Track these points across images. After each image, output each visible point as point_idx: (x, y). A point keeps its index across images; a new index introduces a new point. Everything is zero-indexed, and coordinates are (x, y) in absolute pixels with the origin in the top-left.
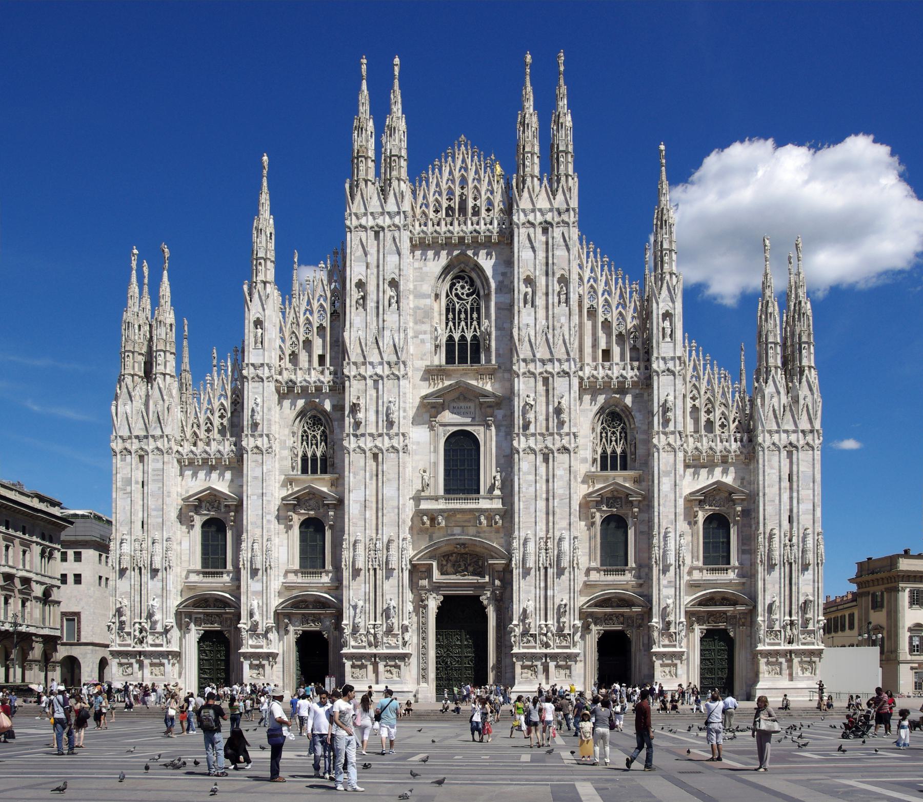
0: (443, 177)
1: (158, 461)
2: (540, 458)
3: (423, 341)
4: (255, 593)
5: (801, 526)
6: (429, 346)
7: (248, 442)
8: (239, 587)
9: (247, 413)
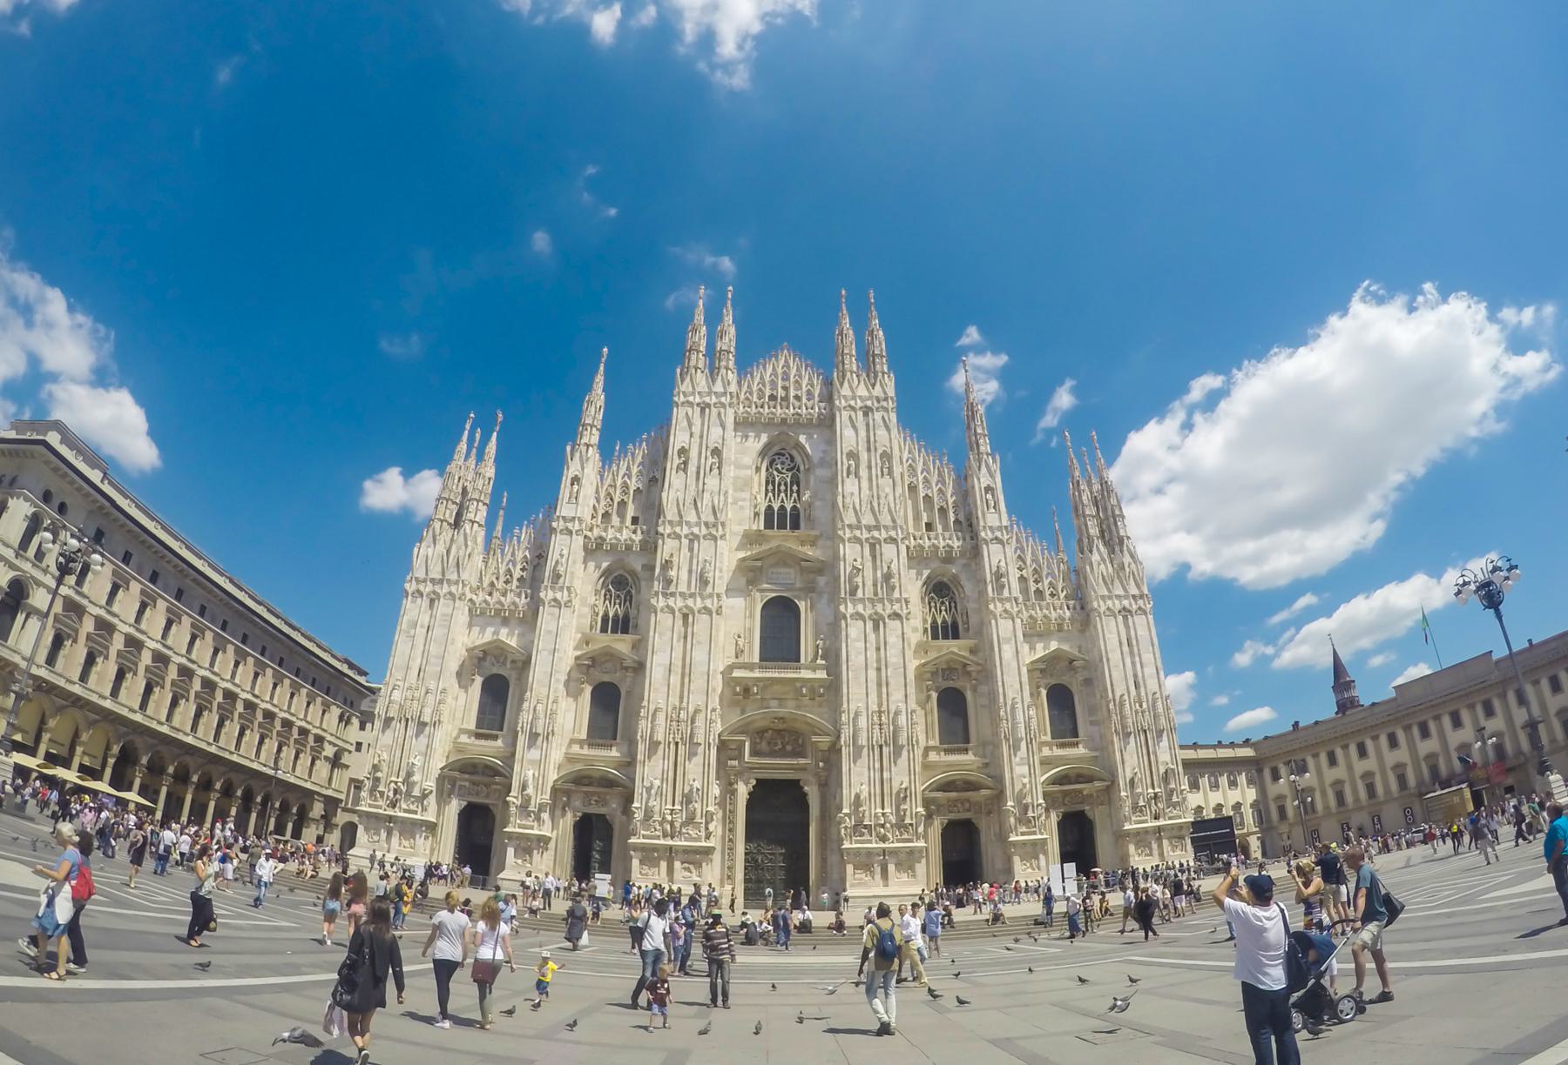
0: (768, 372)
2: (870, 625)
3: (742, 508)
4: (531, 762)
6: (749, 513)
7: (546, 595)
8: (513, 754)
9: (550, 565)
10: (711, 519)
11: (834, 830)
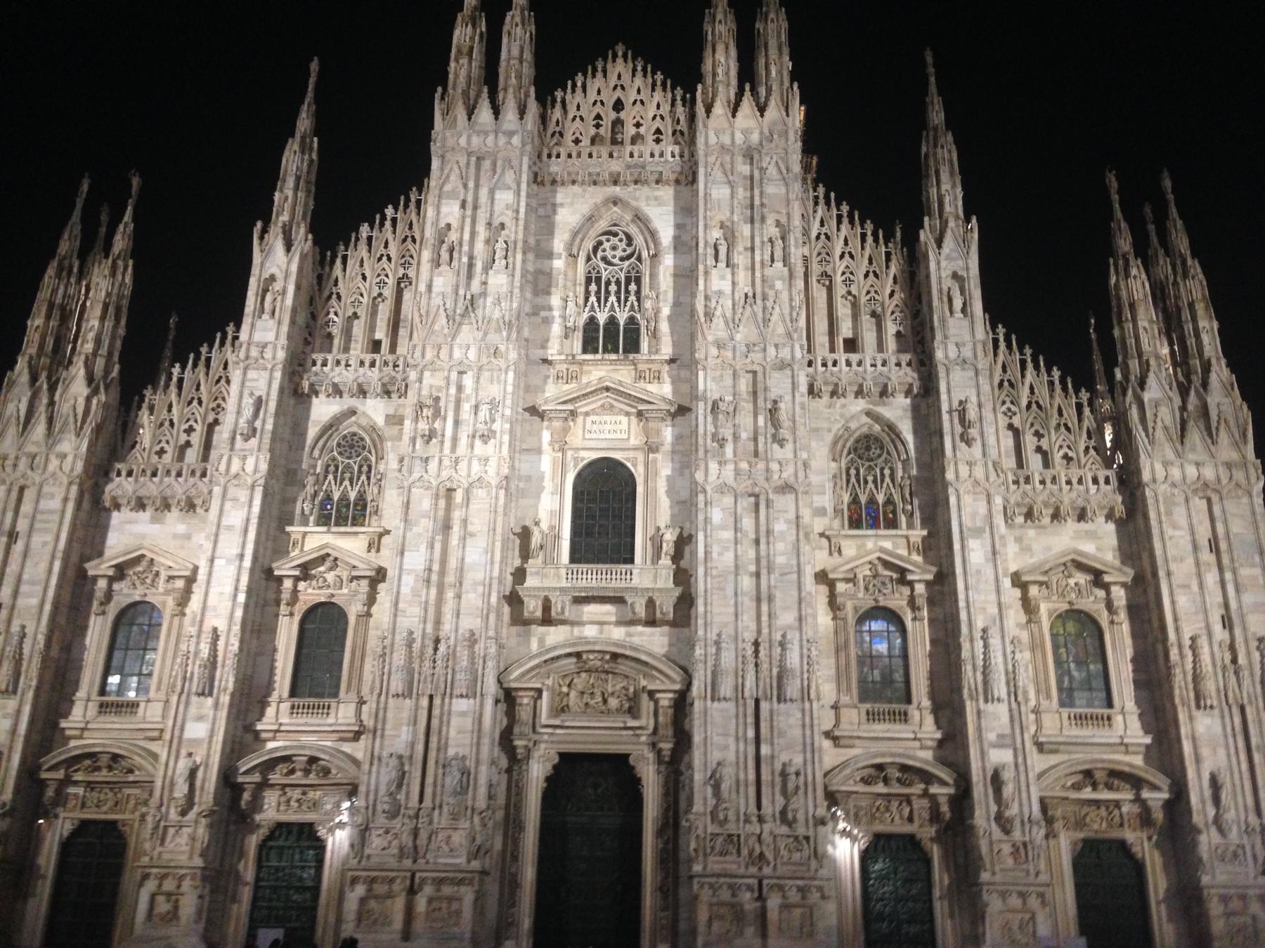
1: (52, 496)
4: (196, 742)
5: (1250, 636)
6: (556, 329)
10: (493, 338)
11: (682, 841)
